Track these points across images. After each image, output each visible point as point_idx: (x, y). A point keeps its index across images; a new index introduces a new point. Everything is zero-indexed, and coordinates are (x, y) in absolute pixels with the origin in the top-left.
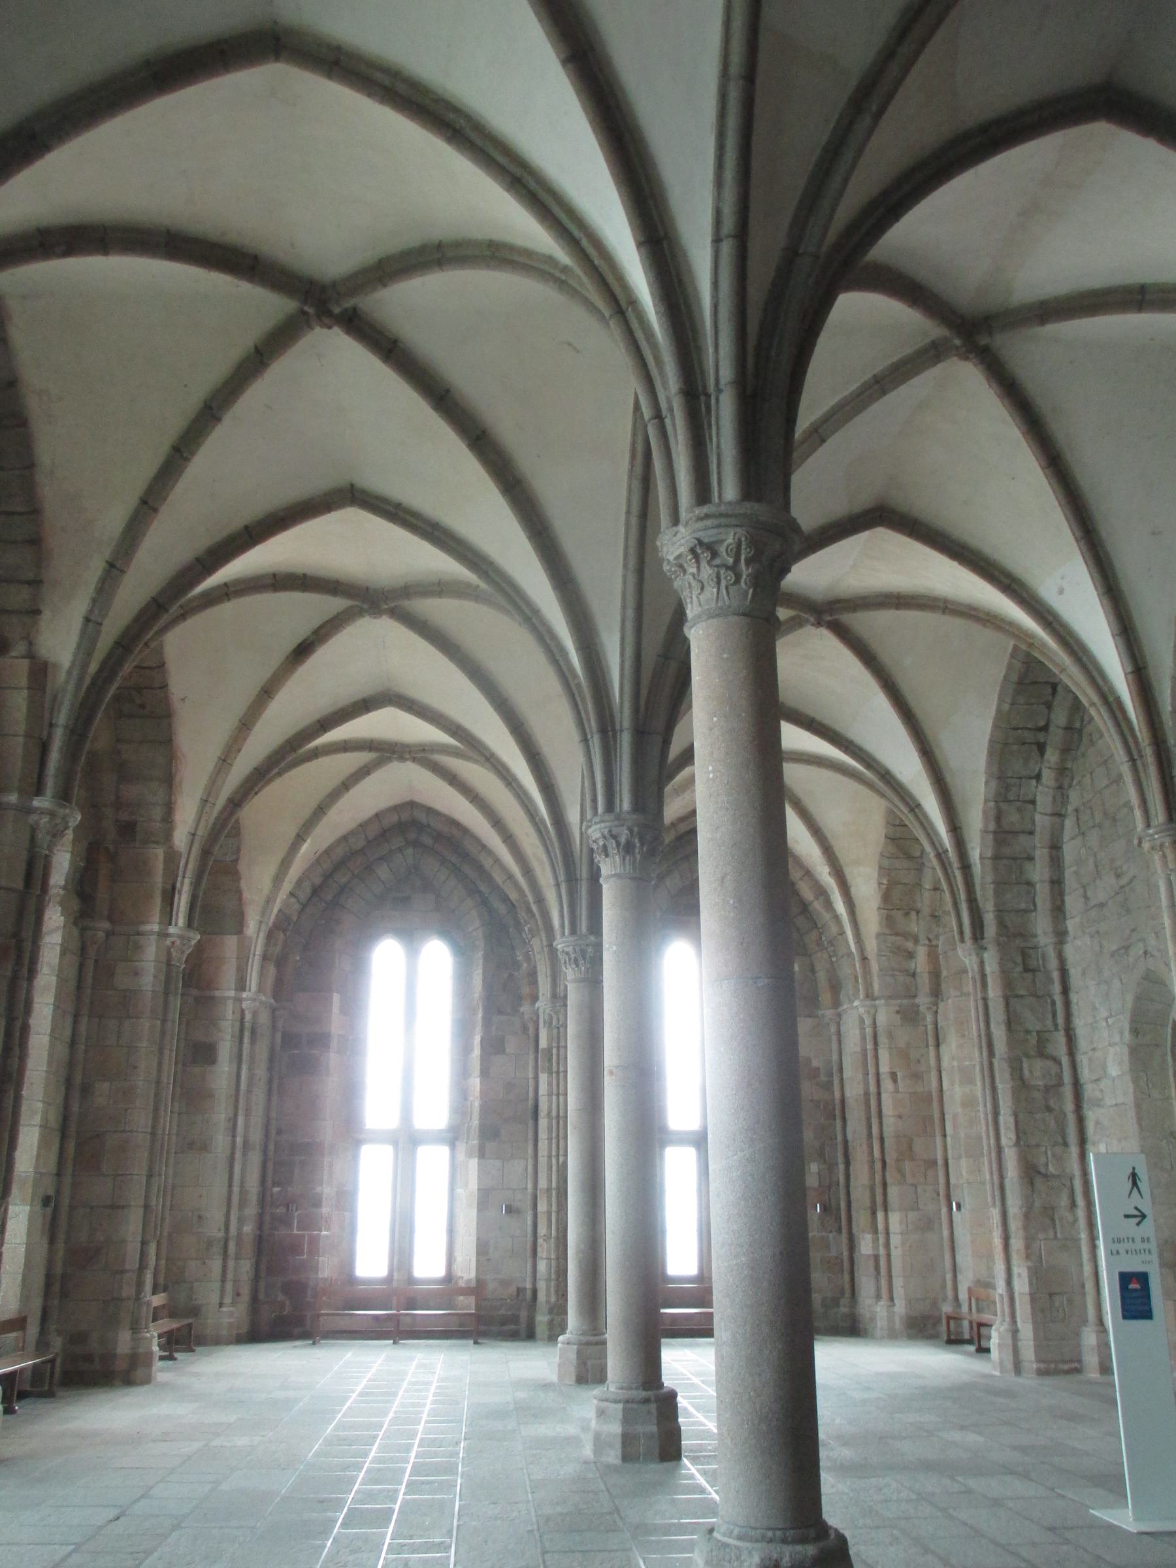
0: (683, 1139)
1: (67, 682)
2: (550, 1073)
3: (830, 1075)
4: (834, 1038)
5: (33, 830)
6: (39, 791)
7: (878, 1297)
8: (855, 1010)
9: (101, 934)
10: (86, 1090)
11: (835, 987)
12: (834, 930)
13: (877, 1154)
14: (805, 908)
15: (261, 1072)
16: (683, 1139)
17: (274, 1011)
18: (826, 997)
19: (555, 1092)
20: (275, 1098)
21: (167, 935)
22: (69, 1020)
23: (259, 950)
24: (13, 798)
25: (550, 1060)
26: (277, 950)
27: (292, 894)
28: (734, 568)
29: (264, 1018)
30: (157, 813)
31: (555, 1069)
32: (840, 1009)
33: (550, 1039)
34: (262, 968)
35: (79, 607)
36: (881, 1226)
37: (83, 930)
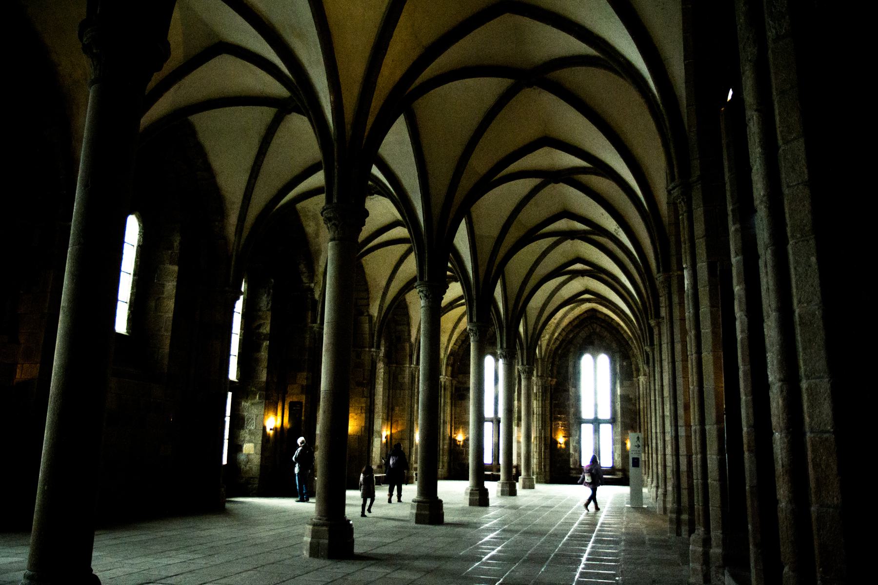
0: (588, 422)
1: (377, 320)
2: (537, 400)
3: (636, 400)
4: (637, 388)
5: (372, 355)
6: (373, 347)
7: (645, 474)
8: (642, 379)
9: (394, 368)
10: (393, 409)
11: (638, 370)
12: (635, 351)
13: (646, 428)
14: (628, 344)
15: (448, 401)
16: (588, 422)
17: (452, 381)
18: (635, 374)
19: (538, 406)
20: (453, 408)
21: (411, 367)
22: (387, 391)
23: (445, 361)
24: (367, 349)
25: (537, 396)
26: (451, 362)
27: (455, 344)
28: (476, 333)
29: (447, 383)
30: (406, 334)
31: (538, 399)
32: (639, 377)
33: (536, 390)
34: (446, 368)
35: (378, 302)
36: (646, 452)
37: (389, 367)
